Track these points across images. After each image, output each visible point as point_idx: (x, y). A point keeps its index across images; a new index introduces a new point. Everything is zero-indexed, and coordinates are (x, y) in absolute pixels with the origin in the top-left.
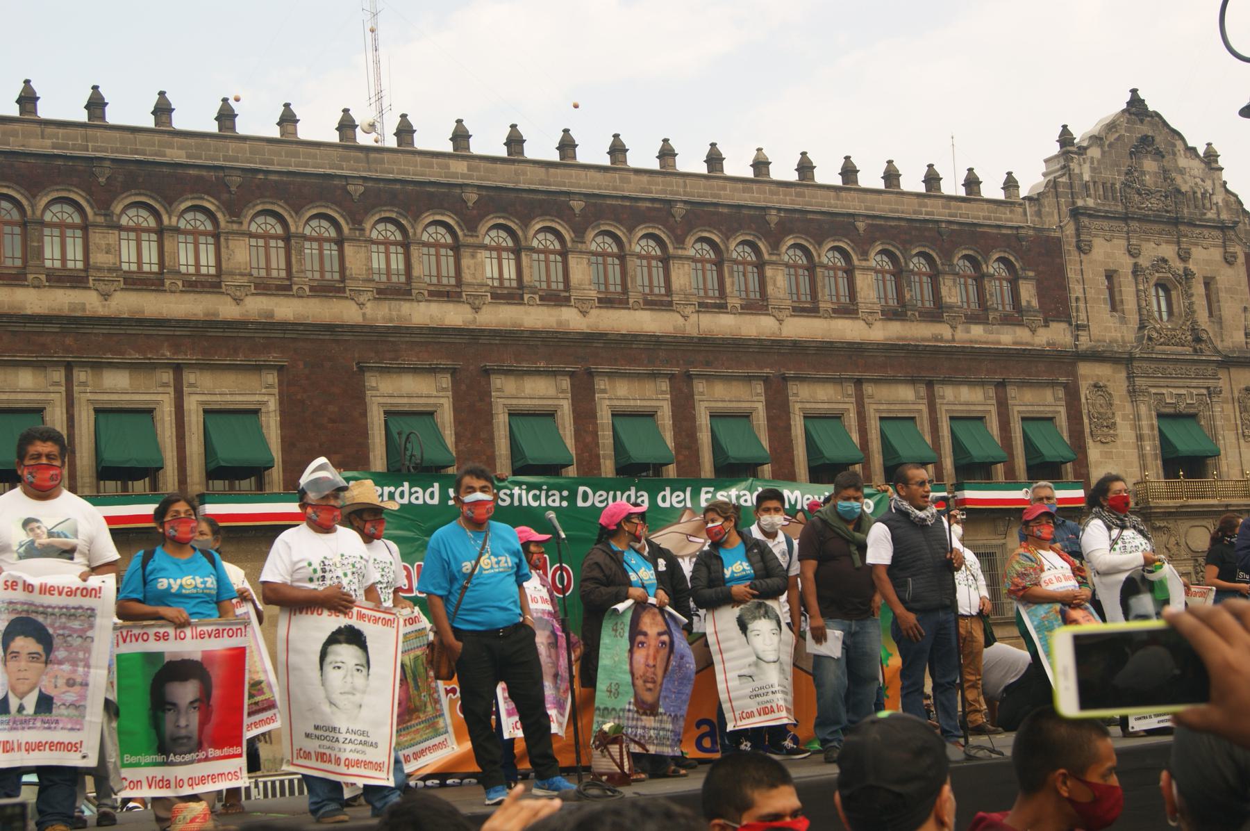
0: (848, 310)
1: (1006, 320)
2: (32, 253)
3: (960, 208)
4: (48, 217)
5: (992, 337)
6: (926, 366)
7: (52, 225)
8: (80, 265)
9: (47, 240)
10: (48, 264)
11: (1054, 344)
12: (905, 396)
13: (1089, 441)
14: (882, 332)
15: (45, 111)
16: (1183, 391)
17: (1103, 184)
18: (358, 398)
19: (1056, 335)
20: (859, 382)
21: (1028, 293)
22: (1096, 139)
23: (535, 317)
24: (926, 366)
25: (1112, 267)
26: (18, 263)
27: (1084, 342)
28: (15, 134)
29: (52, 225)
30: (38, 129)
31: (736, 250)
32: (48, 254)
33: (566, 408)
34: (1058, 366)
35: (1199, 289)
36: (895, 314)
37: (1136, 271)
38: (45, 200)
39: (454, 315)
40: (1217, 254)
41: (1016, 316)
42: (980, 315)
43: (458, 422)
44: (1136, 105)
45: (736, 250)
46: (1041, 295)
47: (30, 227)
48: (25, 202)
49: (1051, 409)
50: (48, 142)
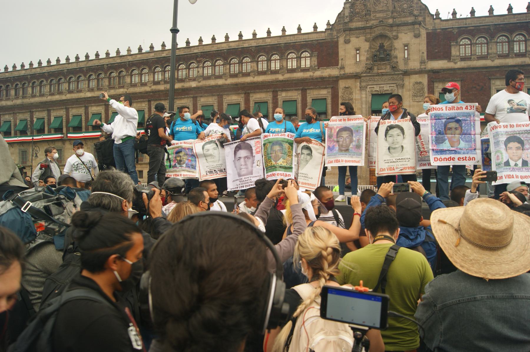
2: (511, 49)
4: (515, 39)
7: (516, 41)
8: (524, 51)
9: (515, 46)
10: (515, 52)
15: (514, 11)
26: (507, 52)
28: (506, 19)
29: (516, 41)
30: (513, 16)
32: (515, 49)
38: (515, 35)
47: (511, 43)
48: (509, 36)
50: (515, 19)
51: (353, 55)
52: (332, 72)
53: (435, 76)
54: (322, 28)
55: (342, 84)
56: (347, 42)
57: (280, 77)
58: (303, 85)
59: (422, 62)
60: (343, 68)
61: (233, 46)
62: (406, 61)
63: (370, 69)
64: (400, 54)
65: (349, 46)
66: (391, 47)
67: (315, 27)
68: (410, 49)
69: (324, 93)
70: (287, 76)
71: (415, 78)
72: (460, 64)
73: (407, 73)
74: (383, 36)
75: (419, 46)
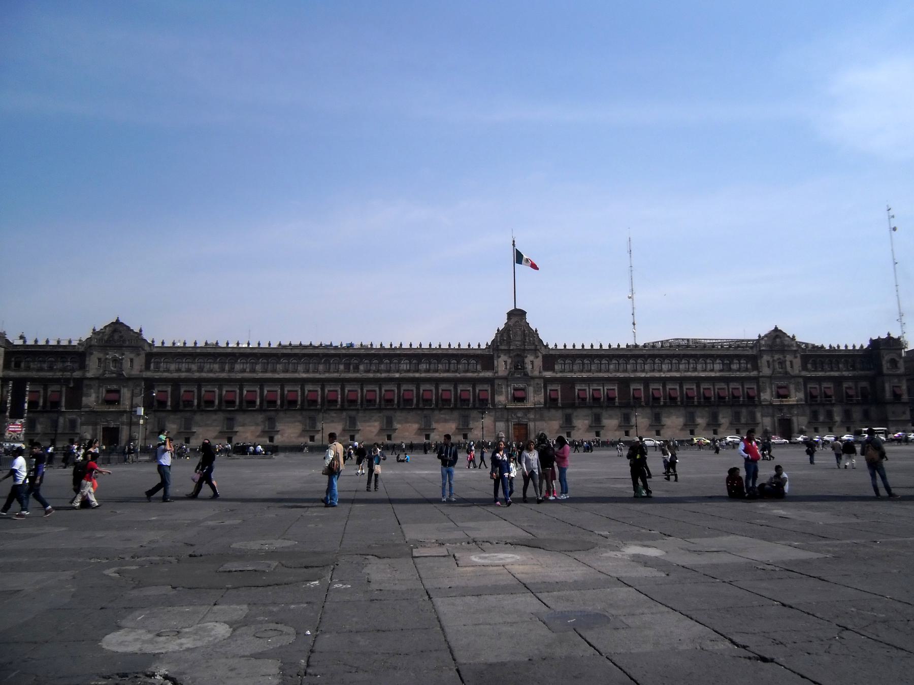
0: (712, 370)
1: (744, 371)
12: (723, 385)
14: (718, 374)
18: (629, 387)
19: (754, 373)
21: (749, 366)
22: (766, 336)
23: (657, 375)
27: (761, 374)
31: (691, 361)
34: (756, 379)
35: (788, 364)
36: (721, 371)
37: (774, 361)
39: (643, 375)
41: (747, 370)
42: (739, 370)
44: (776, 328)
45: (691, 361)
46: (752, 366)
51: (502, 365)
52: (488, 374)
53: (547, 381)
54: (483, 346)
55: (496, 382)
56: (499, 357)
57: (458, 375)
58: (474, 382)
60: (497, 372)
61: (426, 352)
62: (532, 372)
64: (529, 367)
65: (500, 359)
66: (523, 362)
67: (479, 345)
68: (534, 365)
69: (487, 387)
70: (462, 375)
71: (537, 381)
72: (559, 375)
73: (533, 378)
74: (518, 355)
75: (539, 362)
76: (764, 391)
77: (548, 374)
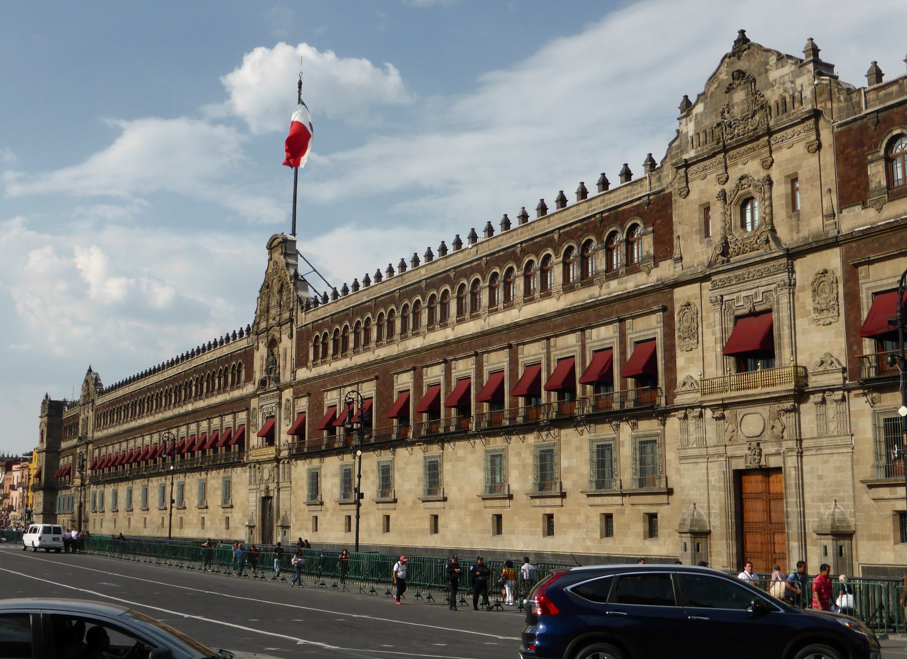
3: (610, 199)
5: (622, 287)
6: (578, 319)
11: (661, 279)
13: (678, 352)
16: (752, 292)
17: (705, 131)
19: (666, 270)
20: (548, 339)
24: (578, 319)
25: (705, 200)
33: (442, 379)
36: (568, 287)
37: (723, 195)
40: (800, 148)
43: (415, 393)
44: (742, 40)
49: (652, 332)
59: (294, 372)
63: (263, 383)
76: (693, 333)
77: (303, 374)
